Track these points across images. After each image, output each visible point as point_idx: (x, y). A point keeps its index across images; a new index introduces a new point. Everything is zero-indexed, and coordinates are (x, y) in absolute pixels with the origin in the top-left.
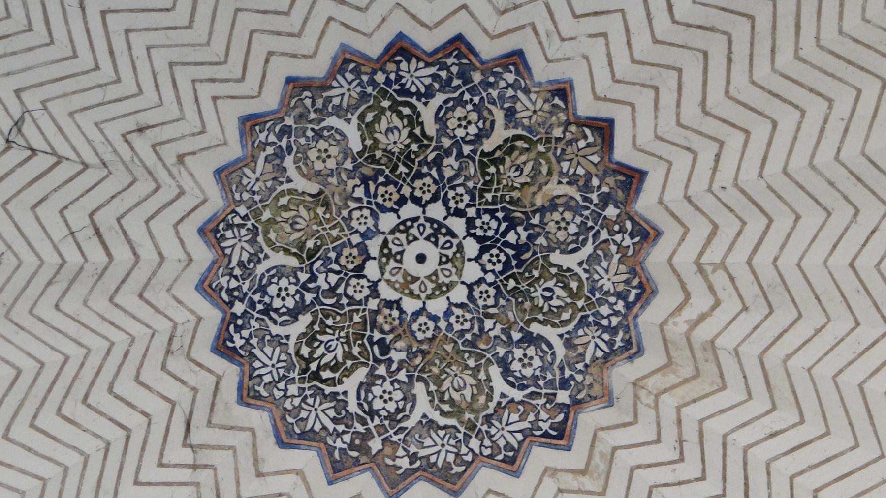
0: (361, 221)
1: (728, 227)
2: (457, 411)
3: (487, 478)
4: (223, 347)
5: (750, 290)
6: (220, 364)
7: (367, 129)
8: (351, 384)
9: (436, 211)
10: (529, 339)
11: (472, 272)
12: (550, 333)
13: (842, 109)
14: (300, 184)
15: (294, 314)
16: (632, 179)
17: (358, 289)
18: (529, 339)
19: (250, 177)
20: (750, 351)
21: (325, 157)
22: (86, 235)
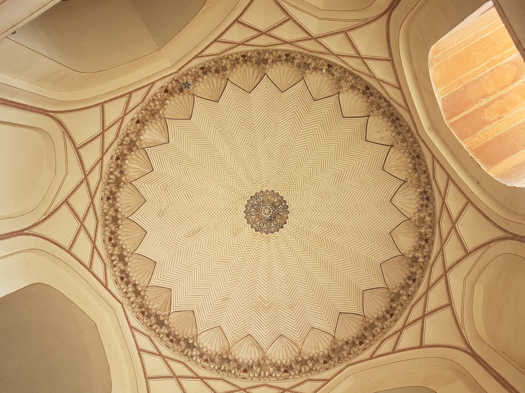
1: (282, 238)
3: (250, 226)
4: (251, 197)
7: (277, 202)
11: (268, 216)
16: (282, 227)
17: (262, 207)
20: (271, 245)
21: (273, 199)
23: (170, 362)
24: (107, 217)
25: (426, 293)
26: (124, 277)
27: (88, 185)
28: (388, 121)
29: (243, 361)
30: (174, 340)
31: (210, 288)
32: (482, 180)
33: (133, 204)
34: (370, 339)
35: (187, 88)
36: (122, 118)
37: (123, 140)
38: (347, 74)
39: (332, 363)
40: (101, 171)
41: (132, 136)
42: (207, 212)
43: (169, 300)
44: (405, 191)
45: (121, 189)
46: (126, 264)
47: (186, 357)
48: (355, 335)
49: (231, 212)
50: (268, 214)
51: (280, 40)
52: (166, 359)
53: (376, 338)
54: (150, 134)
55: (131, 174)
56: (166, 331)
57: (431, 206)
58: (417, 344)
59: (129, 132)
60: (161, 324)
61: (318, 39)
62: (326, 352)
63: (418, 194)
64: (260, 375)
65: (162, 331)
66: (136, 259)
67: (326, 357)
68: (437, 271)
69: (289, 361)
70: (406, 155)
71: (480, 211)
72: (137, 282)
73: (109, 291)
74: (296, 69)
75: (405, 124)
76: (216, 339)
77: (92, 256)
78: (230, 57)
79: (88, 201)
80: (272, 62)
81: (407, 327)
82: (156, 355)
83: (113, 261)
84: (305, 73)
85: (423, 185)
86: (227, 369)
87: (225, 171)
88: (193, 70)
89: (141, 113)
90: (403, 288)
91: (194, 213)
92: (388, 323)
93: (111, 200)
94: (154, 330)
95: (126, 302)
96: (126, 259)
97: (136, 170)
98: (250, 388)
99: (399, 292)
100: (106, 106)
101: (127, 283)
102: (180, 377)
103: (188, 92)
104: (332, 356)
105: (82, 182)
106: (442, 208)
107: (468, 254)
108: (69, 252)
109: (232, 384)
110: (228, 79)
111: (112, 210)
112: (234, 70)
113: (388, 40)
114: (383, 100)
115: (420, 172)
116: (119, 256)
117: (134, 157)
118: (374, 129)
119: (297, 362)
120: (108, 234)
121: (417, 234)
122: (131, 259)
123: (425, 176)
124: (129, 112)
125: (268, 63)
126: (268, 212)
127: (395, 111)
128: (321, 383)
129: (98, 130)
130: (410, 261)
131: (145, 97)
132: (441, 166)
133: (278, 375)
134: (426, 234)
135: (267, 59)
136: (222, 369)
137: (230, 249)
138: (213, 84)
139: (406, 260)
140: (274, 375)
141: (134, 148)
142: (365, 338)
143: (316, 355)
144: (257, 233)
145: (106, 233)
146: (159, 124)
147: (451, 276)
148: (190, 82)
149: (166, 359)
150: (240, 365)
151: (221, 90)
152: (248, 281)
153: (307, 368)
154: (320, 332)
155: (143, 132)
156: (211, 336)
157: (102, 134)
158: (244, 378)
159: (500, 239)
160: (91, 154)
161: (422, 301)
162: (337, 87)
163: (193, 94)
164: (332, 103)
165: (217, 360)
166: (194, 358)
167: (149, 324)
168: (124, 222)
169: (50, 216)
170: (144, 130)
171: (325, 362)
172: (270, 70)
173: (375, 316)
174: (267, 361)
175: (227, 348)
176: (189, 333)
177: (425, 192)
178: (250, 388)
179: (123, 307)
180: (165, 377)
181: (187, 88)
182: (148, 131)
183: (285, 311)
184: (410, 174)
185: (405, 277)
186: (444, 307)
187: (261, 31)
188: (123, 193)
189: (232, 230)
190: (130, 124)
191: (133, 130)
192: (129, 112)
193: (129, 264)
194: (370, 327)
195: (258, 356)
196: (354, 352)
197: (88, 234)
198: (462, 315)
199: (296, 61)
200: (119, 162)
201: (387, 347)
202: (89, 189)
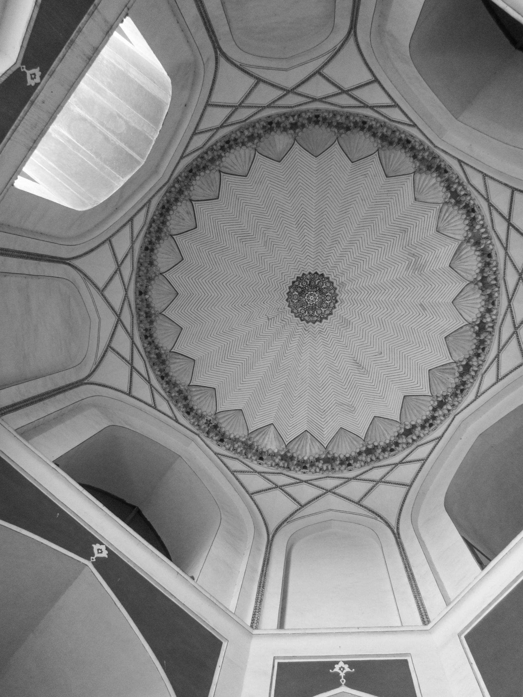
0: (304, 299)
2: (326, 307)
3: (334, 311)
4: (302, 320)
5: (341, 274)
6: (303, 322)
7: (297, 292)
8: (315, 314)
9: (309, 293)
11: (317, 295)
12: (328, 294)
13: (334, 252)
14: (296, 301)
15: (305, 312)
16: (322, 275)
18: (327, 296)
19: (291, 304)
20: (346, 279)
22: (282, 322)
23: (502, 343)
24: (369, 460)
25: (321, 100)
26: (429, 423)
27: (336, 487)
28: (169, 215)
29: (480, 262)
30: (482, 347)
31: (416, 329)
32: (180, 105)
33: (348, 440)
34: (399, 134)
35: (211, 422)
36: (259, 473)
37: (284, 467)
38: (141, 273)
39: (443, 164)
40: (320, 478)
43: (441, 368)
44: (230, 167)
45: (336, 455)
46: (414, 427)
47: (495, 327)
48: (403, 151)
49: (326, 337)
50: (315, 295)
51: (132, 349)
52: (501, 348)
53: (395, 129)
54: (270, 444)
55: (317, 450)
56: (475, 359)
57: (233, 136)
58: (376, 85)
59: (274, 464)
60: (467, 368)
61: (118, 314)
62: (435, 175)
63: (227, 154)
64: (487, 238)
65: (475, 364)
66: (406, 418)
67: (441, 173)
68: (292, 100)
69: (461, 212)
70: (194, 182)
71: (212, 89)
72: (431, 408)
73: (444, 434)
74: (155, 324)
75: (165, 198)
77: (410, 462)
78: (168, 390)
79: (354, 483)
81: (365, 104)
83: (414, 440)
84: (155, 314)
85: (215, 153)
86: (493, 277)
87: (284, 358)
88: (192, 421)
89: (251, 457)
90: (330, 125)
91: (340, 375)
92: (374, 123)
94: (476, 372)
95: (453, 413)
96: (408, 428)
98: (502, 244)
99: (336, 127)
100: (251, 490)
102: (514, 325)
103: (215, 419)
104: (435, 167)
105: (334, 493)
107: (259, 80)
108: (410, 486)
109: (505, 264)
110: (189, 385)
111: (360, 458)
112: (178, 382)
113: (92, 250)
114: (152, 229)
115: (204, 162)
116: (407, 436)
117: (299, 452)
118: (182, 224)
119: (458, 202)
120: (386, 454)
121: (267, 135)
122: (407, 423)
123: (205, 156)
124: (252, 469)
125: (159, 353)
126: (311, 295)
127: (157, 213)
128: (465, 167)
129: (278, 492)
130: (297, 131)
131: (232, 458)
132: (187, 146)
133: (480, 217)
134: (264, 127)
135: (157, 354)
136: (494, 282)
137: (367, 322)
138: (199, 398)
139: (300, 134)
140: (481, 222)
141: (289, 455)
142: (400, 140)
143: (443, 184)
144: (339, 300)
145: (386, 456)
146: (257, 438)
147: (290, 84)
148: (205, 421)
149: (501, 348)
150: (485, 264)
151: (203, 389)
153: (460, 188)
154: (416, 190)
155: (270, 452)
156: (465, 307)
157: (281, 487)
158: (496, 254)
159: (228, 59)
160: (305, 492)
161: (330, 100)
162: (157, 278)
163: (215, 414)
164: (174, 276)
165: (489, 291)
166: (494, 317)
167: (472, 381)
168: (370, 442)
169: (376, 514)
170: (268, 451)
171: (446, 172)
172: (165, 348)
173: (372, 139)
174: (470, 235)
176: (470, 333)
178: (502, 244)
179: (458, 413)
182: (268, 447)
184: (210, 171)
185: (317, 127)
187: (131, 369)
188: (340, 453)
189: (345, 328)
190: (265, 466)
191: (271, 461)
192: (252, 469)
193: (413, 423)
194: (386, 140)
195: (469, 248)
198: (323, 55)
199: (148, 327)
200: (308, 465)
201: (395, 114)
202: (341, 485)
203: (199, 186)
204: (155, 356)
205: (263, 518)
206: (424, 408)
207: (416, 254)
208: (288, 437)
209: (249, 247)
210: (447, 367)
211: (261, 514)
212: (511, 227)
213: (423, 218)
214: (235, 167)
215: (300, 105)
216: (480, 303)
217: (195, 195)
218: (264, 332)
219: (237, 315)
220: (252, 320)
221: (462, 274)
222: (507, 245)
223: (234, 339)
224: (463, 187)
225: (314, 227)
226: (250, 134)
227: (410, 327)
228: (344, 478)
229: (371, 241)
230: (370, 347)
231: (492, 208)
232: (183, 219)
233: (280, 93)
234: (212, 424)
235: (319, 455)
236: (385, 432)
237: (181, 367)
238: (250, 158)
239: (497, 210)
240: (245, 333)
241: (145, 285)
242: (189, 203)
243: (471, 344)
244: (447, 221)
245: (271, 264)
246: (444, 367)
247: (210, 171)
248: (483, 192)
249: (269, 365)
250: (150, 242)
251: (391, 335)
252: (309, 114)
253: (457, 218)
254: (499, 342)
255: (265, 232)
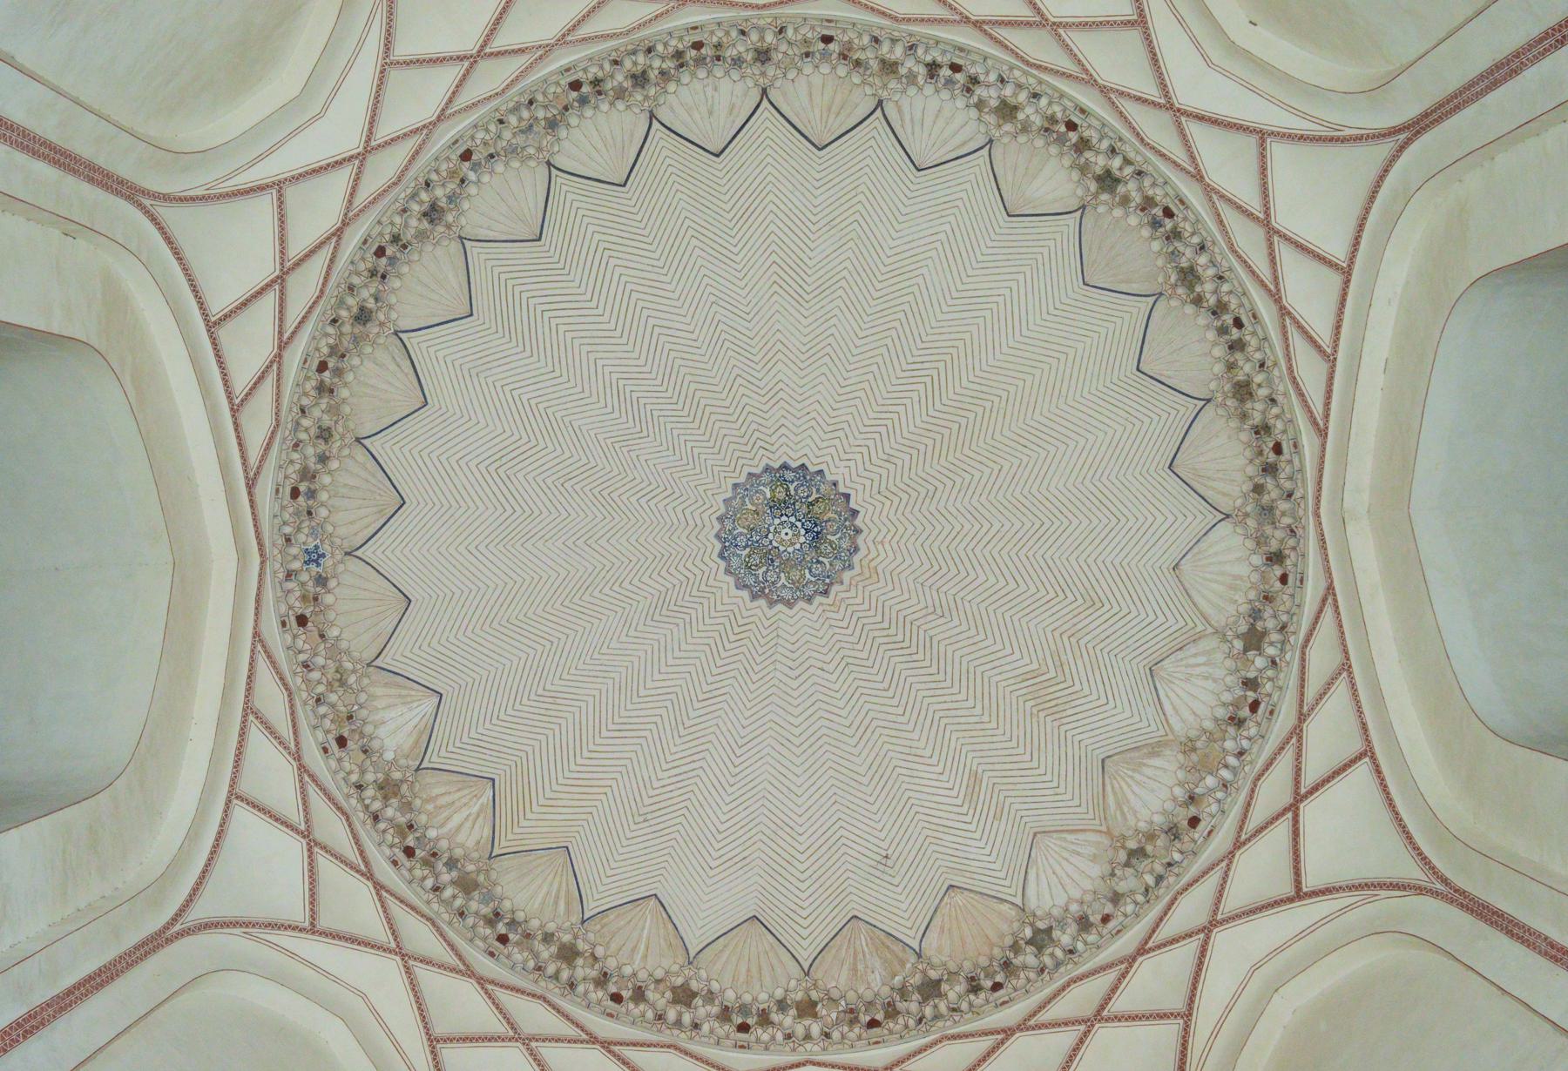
0: (769, 520)
3: (801, 604)
4: (721, 556)
8: (761, 571)
9: (793, 519)
10: (818, 562)
11: (802, 539)
16: (855, 513)
17: (765, 542)
18: (818, 562)
19: (734, 503)
23: (1044, 1017)
24: (551, 969)
25: (1209, 191)
29: (1164, 813)
31: (915, 809)
33: (555, 886)
35: (322, 561)
40: (413, 908)
41: (370, 777)
42: (697, 705)
44: (907, 118)
49: (732, 638)
50: (797, 535)
52: (1032, 1022)
55: (470, 843)
56: (961, 987)
58: (1336, 279)
59: (354, 778)
60: (931, 989)
63: (929, 90)
65: (952, 995)
72: (779, 993)
76: (1064, 863)
80: (377, 300)
82: (1002, 1042)
83: (678, 1023)
85: (910, 63)
86: (1159, 868)
87: (606, 591)
93: (511, 936)
97: (468, 824)
101: (764, 1019)
102: (1102, 1007)
106: (991, 37)
109: (1205, 873)
117: (430, 807)
118: (697, 116)
122: (703, 974)
130: (1105, 197)
133: (1253, 731)
134: (1052, 120)
135: (362, 309)
138: (352, 487)
144: (832, 595)
145: (593, 996)
146: (379, 691)
147: (1185, 97)
149: (1032, 1022)
152: (956, 690)
153: (1275, 637)
154: (1195, 550)
155: (375, 744)
163: (348, 554)
166: (1080, 946)
167: (911, 1022)
172: (394, 315)
175: (1106, 841)
177: (933, 68)
178: (1241, 828)
179: (819, 1064)
180: (1076, 1049)
181: (322, 561)
183: (1092, 626)
184: (864, 82)
186: (1263, 156)
191: (354, 767)
193: (715, 986)
194: (1242, 401)
195: (1173, 767)
196: (1290, 478)
197: (558, 1040)
203: (810, 85)
204: (355, 310)
205: (204, 872)
206: (767, 980)
207: (1066, 668)
208: (443, 753)
209: (777, 307)
210: (894, 948)
211: (210, 859)
212: (1290, 815)
213: (1152, 617)
214: (917, 129)
215: (1163, 155)
216: (1085, 892)
217: (784, 94)
218: (624, 497)
219: (609, 409)
220: (625, 450)
221: (1111, 800)
222: (1249, 840)
223: (551, 448)
224: (1283, 643)
225: (938, 406)
226: (1012, 101)
227: (909, 794)
228: (460, 957)
229: (1013, 554)
230: (794, 749)
231: (1294, 740)
232: (710, 113)
233: (1152, 92)
234: (318, 565)
235: (466, 857)
236: (642, 947)
237: (385, 386)
238: (964, 143)
239: (1299, 756)
240: (584, 461)
241: (492, 151)
242: (755, 95)
243: (986, 949)
244: (1189, 670)
245: (781, 385)
246: (888, 942)
247: (864, 82)
248: (1311, 693)
249: (563, 573)
250: (596, 82)
251: (856, 768)
252: (1159, 191)
253: (1210, 685)
254: (1041, 1007)
255: (836, 311)
